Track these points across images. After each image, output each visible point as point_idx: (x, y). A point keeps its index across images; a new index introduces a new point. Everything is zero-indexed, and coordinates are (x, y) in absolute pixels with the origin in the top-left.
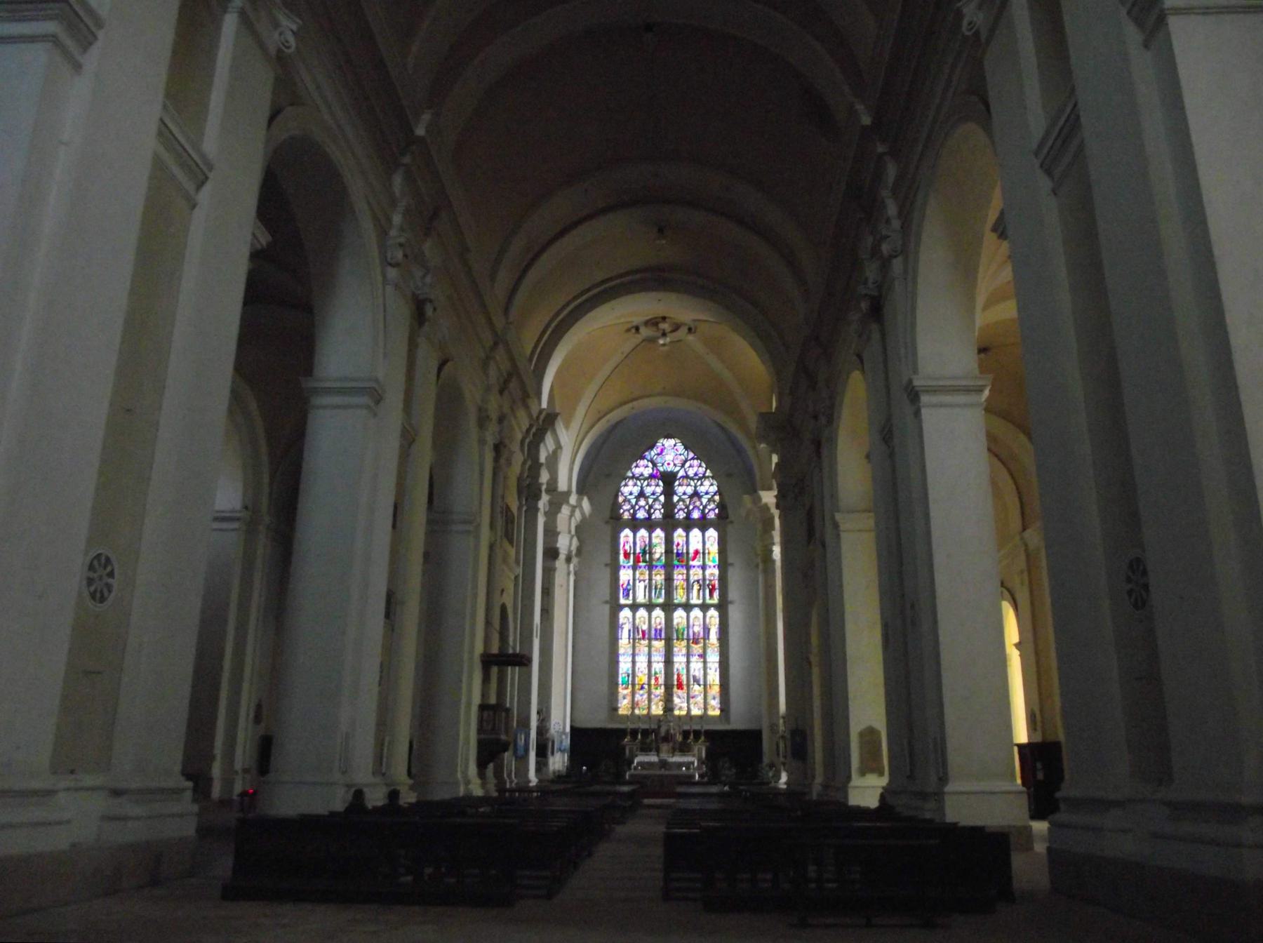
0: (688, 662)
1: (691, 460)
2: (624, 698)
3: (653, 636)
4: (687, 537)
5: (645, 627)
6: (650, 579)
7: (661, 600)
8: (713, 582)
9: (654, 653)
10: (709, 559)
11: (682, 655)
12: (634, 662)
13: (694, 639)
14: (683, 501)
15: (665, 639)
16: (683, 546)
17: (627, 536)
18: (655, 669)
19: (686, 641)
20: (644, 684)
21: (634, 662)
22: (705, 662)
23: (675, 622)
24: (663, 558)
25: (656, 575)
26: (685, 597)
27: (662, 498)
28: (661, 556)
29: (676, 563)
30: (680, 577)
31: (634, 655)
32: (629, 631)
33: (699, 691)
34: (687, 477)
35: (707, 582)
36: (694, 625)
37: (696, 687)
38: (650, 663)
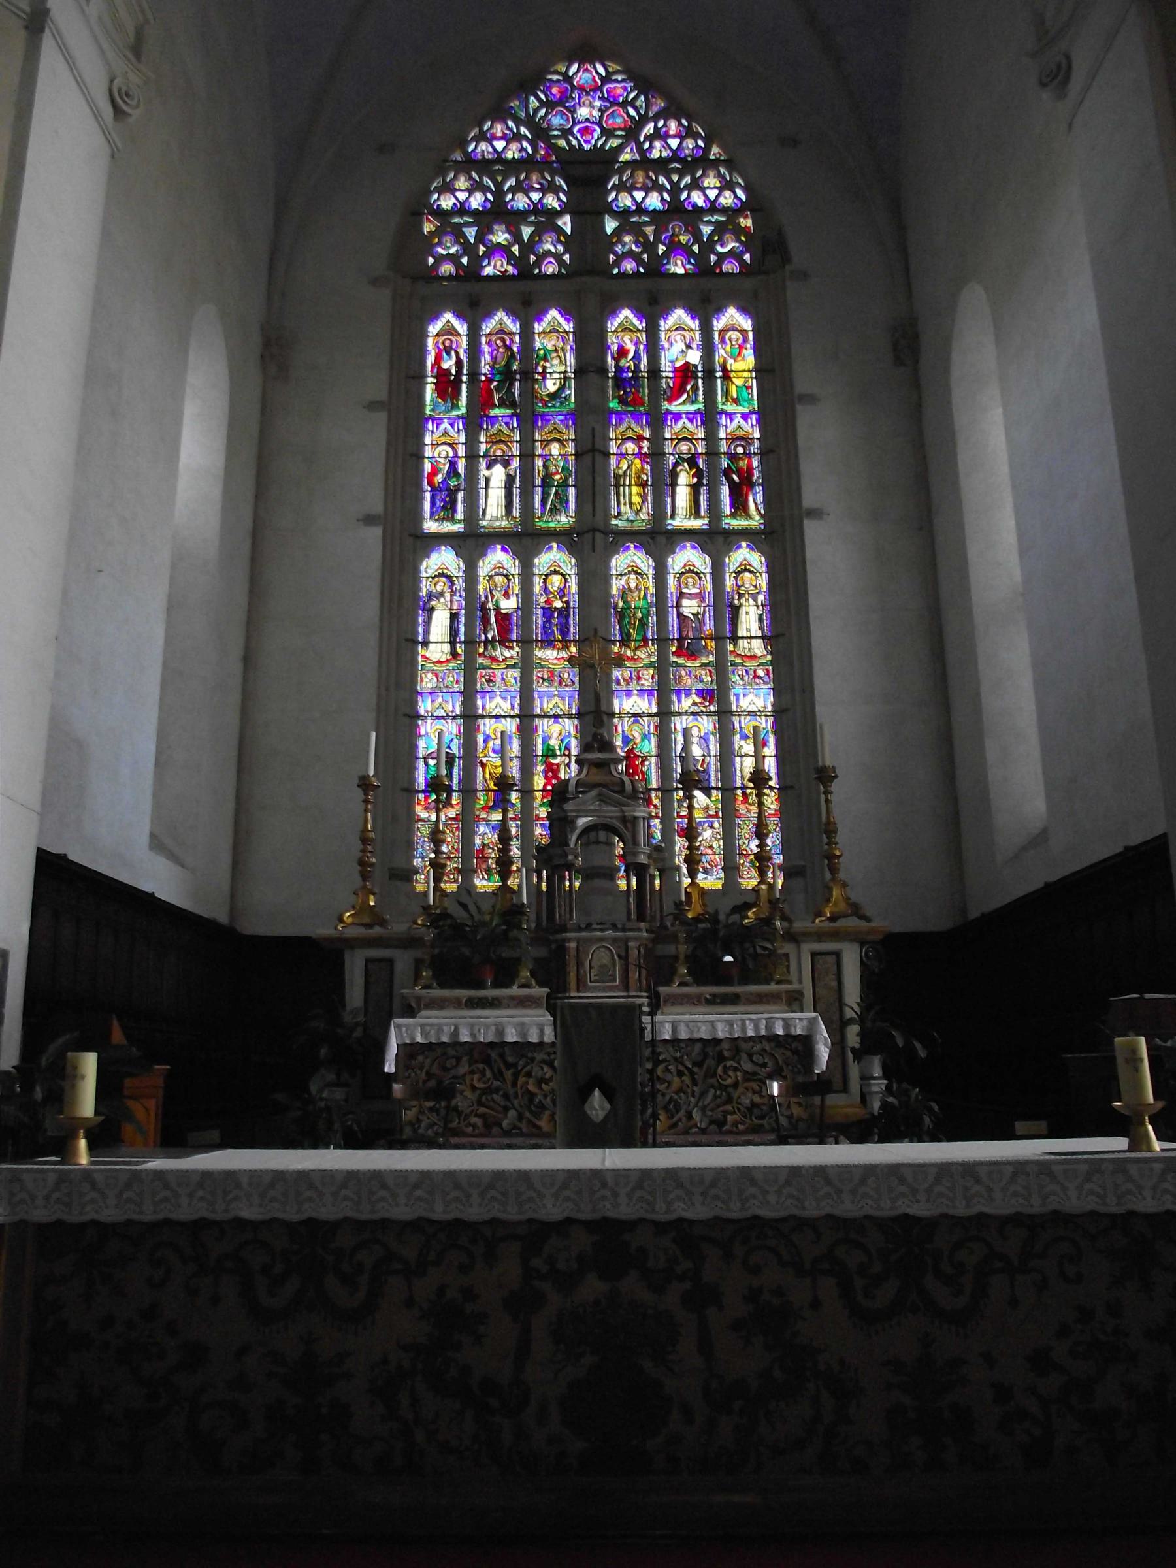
0: (664, 714)
1: (655, 119)
3: (537, 633)
4: (652, 332)
5: (509, 605)
6: (527, 456)
7: (564, 520)
8: (742, 464)
9: (540, 687)
10: (726, 394)
11: (641, 692)
12: (470, 718)
13: (681, 640)
16: (637, 357)
17: (450, 331)
18: (545, 739)
19: (652, 648)
21: (470, 718)
22: (724, 714)
23: (616, 586)
24: (571, 392)
25: (546, 443)
26: (647, 508)
27: (566, 223)
28: (562, 388)
29: (613, 404)
30: (630, 447)
31: (469, 695)
32: (454, 617)
33: (706, 808)
34: (644, 162)
35: (724, 463)
36: (681, 596)
38: (526, 718)
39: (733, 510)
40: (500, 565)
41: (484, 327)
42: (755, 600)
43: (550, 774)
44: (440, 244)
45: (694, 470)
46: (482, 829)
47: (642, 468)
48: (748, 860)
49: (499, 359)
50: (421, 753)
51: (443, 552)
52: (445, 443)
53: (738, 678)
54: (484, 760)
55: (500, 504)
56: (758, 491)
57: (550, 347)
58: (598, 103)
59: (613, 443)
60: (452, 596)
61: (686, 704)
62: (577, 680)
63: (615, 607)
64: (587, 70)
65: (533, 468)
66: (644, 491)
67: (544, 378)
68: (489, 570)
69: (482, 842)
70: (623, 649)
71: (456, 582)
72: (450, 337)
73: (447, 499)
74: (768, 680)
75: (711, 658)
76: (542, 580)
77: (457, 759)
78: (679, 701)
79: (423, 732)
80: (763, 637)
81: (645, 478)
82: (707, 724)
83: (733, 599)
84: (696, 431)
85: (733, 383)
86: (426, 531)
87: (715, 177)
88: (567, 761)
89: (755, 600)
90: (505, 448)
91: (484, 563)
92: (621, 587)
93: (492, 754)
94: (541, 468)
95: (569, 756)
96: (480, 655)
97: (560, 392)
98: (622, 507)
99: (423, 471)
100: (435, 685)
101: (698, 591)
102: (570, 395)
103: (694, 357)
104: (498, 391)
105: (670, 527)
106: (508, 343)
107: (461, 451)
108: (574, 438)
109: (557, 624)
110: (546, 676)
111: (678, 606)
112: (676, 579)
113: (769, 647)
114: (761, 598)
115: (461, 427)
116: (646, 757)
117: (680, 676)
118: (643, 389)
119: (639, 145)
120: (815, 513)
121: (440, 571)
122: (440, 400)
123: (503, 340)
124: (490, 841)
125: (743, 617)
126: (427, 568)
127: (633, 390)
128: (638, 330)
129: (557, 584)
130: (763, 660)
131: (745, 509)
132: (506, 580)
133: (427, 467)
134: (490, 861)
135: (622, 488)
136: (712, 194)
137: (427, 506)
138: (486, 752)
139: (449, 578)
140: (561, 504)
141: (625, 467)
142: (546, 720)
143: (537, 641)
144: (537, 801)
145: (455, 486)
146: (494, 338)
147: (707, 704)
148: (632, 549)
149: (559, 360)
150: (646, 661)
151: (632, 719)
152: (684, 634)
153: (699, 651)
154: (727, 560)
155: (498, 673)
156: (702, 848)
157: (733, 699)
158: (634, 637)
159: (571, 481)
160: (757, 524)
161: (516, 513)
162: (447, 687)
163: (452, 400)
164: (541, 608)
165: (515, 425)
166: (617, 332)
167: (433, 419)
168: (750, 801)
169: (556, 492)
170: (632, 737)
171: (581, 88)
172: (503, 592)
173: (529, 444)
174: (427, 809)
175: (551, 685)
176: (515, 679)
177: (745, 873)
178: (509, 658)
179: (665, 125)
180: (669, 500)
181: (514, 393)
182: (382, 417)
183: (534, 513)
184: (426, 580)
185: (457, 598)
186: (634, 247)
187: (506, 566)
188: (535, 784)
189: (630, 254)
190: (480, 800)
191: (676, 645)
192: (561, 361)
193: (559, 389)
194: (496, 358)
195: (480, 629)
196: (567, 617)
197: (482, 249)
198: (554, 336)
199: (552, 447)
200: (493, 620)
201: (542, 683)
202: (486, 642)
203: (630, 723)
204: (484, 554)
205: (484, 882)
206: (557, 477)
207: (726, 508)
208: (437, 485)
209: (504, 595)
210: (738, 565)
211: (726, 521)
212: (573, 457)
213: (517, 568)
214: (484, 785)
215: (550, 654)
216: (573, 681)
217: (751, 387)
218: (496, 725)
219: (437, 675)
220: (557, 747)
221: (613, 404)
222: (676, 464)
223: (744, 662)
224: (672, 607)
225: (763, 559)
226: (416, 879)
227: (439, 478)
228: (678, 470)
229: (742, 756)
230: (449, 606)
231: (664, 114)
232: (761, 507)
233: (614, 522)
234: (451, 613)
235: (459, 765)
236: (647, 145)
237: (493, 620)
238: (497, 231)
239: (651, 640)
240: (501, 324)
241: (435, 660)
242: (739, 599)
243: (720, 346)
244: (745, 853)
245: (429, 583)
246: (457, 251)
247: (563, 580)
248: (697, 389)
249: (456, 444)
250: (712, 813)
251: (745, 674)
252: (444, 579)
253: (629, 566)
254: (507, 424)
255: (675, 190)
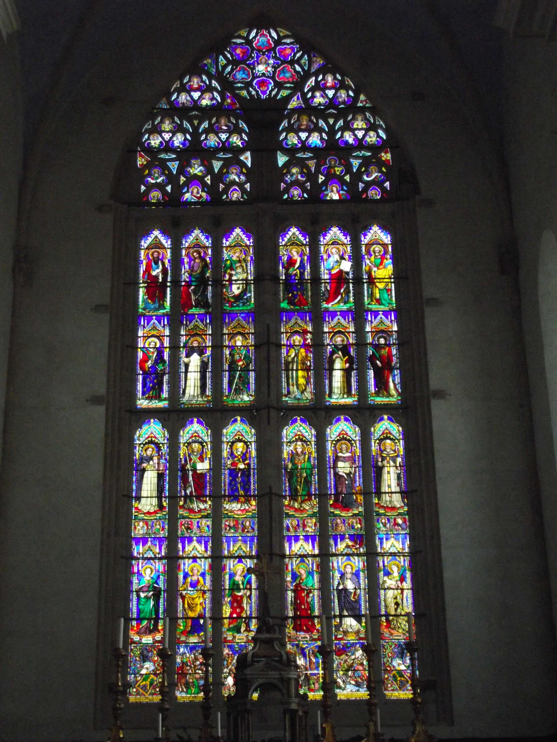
1: (316, 74)
2: (145, 658)
3: (225, 489)
4: (314, 246)
5: (203, 466)
6: (218, 347)
8: (384, 352)
10: (371, 295)
11: (306, 538)
13: (337, 494)
14: (302, 163)
15: (259, 497)
16: (302, 267)
17: (157, 245)
19: (315, 501)
20: (202, 616)
23: (286, 451)
24: (251, 295)
25: (232, 336)
27: (247, 158)
28: (244, 292)
29: (284, 305)
30: (297, 339)
32: (160, 477)
33: (358, 632)
37: (350, 623)
39: (377, 389)
40: (197, 434)
41: (184, 242)
42: (395, 462)
43: (235, 605)
44: (150, 175)
45: (347, 357)
46: (182, 650)
47: (307, 356)
48: (391, 675)
49: (195, 268)
50: (135, 587)
51: (152, 424)
52: (153, 336)
53: (381, 525)
54: (184, 593)
55: (196, 385)
56: (396, 373)
57: (234, 258)
58: (271, 61)
59: (284, 336)
60: (159, 459)
61: (341, 546)
62: (256, 527)
63: (286, 469)
64: (263, 35)
65: (222, 356)
66: (308, 374)
67: (231, 284)
68: (188, 438)
69: (182, 661)
70: (292, 502)
71: (162, 448)
72: (157, 250)
73: (155, 381)
74: (405, 526)
75: (361, 509)
76: (229, 447)
77: (162, 592)
78: (336, 544)
79: (136, 570)
80: (401, 492)
81: (309, 364)
82: (358, 563)
83: (377, 461)
84: (348, 326)
85: (376, 286)
86: (139, 407)
87: (362, 121)
88: (248, 594)
89: (395, 462)
90: (200, 340)
91: (184, 432)
92: (290, 452)
93: (190, 589)
94: (228, 356)
95: (250, 589)
96: (182, 507)
97: (242, 295)
98: (291, 387)
99: (137, 358)
100: (145, 532)
101: (350, 455)
102: (250, 297)
103: (346, 266)
104: (195, 294)
105: (328, 403)
106: (202, 255)
107: (166, 343)
108: (253, 331)
109: (240, 482)
110: (232, 525)
111: (335, 467)
112: (333, 445)
113: (406, 500)
114: (399, 460)
115: (166, 323)
116: (310, 590)
117: (337, 524)
118: (307, 291)
119: (304, 95)
120: (440, 394)
121: (150, 439)
122: (150, 301)
123: (199, 253)
124: (188, 660)
125: (385, 476)
126: (139, 436)
128: (303, 245)
129: (240, 450)
130: (401, 511)
131: (387, 388)
132: (201, 447)
133: (140, 355)
134: (188, 676)
135: (290, 372)
136: (360, 134)
137: (140, 387)
138: (185, 586)
139: (157, 445)
140: (244, 384)
141: (293, 355)
142: (232, 560)
143: (225, 496)
144: (225, 626)
145: (161, 370)
146: (192, 251)
147: (358, 546)
148: (299, 421)
150: (310, 512)
151: (299, 559)
152: (340, 489)
153: (351, 504)
154: (372, 429)
155: (195, 523)
156: (355, 665)
157: (378, 542)
158: (301, 492)
159: (251, 367)
160: (395, 400)
161: (208, 392)
162: (155, 533)
163: (159, 301)
164: (228, 469)
165: (208, 321)
166: (287, 246)
167: (145, 316)
168: (392, 626)
169: (240, 375)
170: (299, 574)
171: (259, 50)
172: (198, 456)
174: (138, 633)
175: (236, 531)
176: (208, 526)
177: (389, 685)
178: (204, 510)
179: (323, 79)
180: (327, 382)
181: (207, 295)
182: (106, 317)
183: (222, 392)
184: (139, 446)
185: (163, 461)
186: (299, 177)
187: (201, 435)
188: (224, 612)
189: (296, 183)
190: (180, 625)
191: (333, 499)
192: (243, 269)
193: (242, 292)
194: (193, 267)
195: (181, 487)
196: (249, 476)
197: (183, 179)
198: (238, 249)
199: (237, 339)
200: (191, 478)
201: (229, 530)
202: (186, 496)
203: (297, 562)
204: (184, 426)
205: (184, 695)
207: (372, 389)
208: (147, 369)
209: (199, 459)
210: (381, 433)
211: (372, 398)
212: (253, 348)
213: (209, 437)
214: (183, 613)
215: (236, 506)
216: (253, 529)
217: (391, 290)
218: (193, 564)
219: (147, 524)
220: (240, 583)
221: (284, 305)
222: (332, 353)
223: (387, 512)
224: (330, 468)
225: (400, 429)
226: (129, 691)
227: (149, 364)
228: (334, 357)
229: (385, 589)
230: (157, 467)
231: (323, 70)
232: (398, 387)
233: (284, 399)
234: (158, 474)
235: (164, 597)
236: (309, 95)
237: (191, 478)
238: (194, 164)
239: (314, 495)
240: (197, 239)
241: (145, 511)
242: (382, 461)
243: (366, 257)
244: (389, 669)
245: (141, 449)
246: (163, 180)
247: (245, 446)
248: (349, 292)
249: (162, 336)
250: (362, 636)
251: (387, 522)
252: (153, 446)
253: (296, 435)
255: (332, 132)
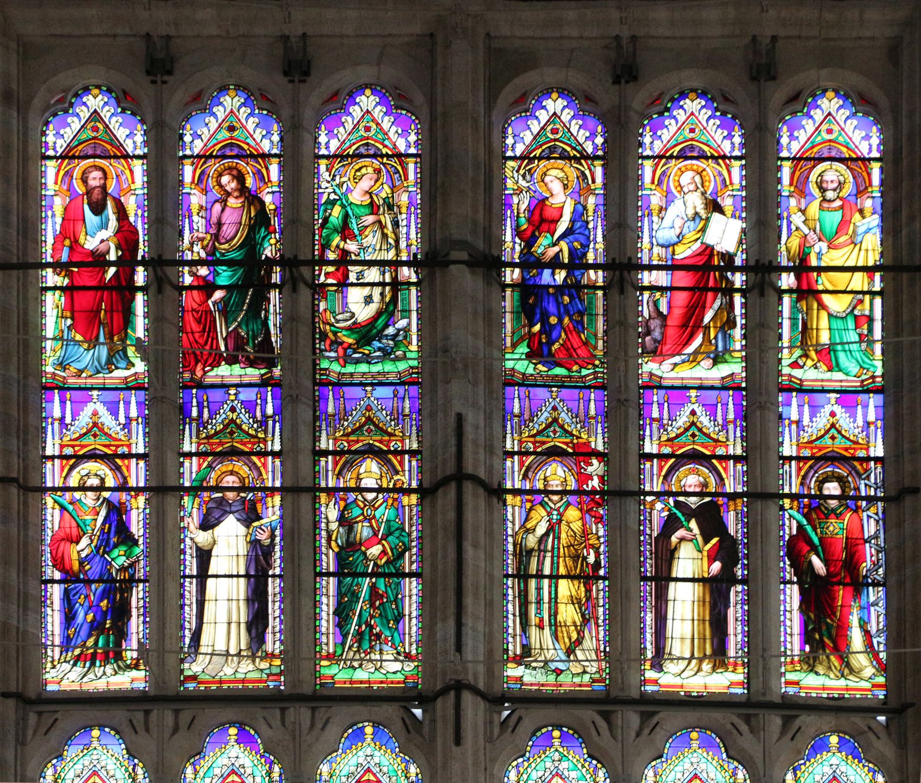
28: (388, 311)
47: (585, 533)
56: (872, 599)
65: (316, 525)
84: (722, 438)
94: (334, 526)
98: (534, 632)
102: (407, 330)
115: (134, 413)
118: (593, 316)
122: (79, 337)
127: (566, 320)
135: (533, 583)
141: (541, 530)
149: (379, 235)
160: (867, 685)
163: (110, 336)
165: (270, 410)
166: (531, 160)
169: (373, 588)
173: (305, 459)
180: (649, 618)
193: (379, 314)
198: (369, 166)
206: (375, 550)
211: (790, 676)
222: (671, 524)
249: (124, 456)
254: (249, 406)
